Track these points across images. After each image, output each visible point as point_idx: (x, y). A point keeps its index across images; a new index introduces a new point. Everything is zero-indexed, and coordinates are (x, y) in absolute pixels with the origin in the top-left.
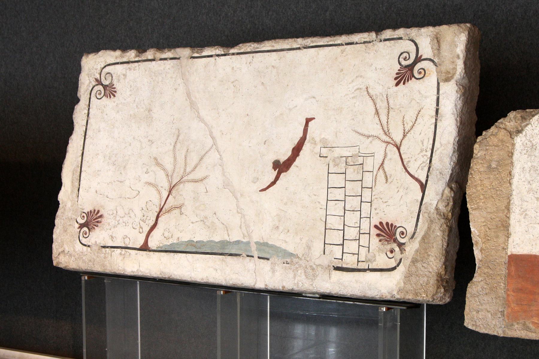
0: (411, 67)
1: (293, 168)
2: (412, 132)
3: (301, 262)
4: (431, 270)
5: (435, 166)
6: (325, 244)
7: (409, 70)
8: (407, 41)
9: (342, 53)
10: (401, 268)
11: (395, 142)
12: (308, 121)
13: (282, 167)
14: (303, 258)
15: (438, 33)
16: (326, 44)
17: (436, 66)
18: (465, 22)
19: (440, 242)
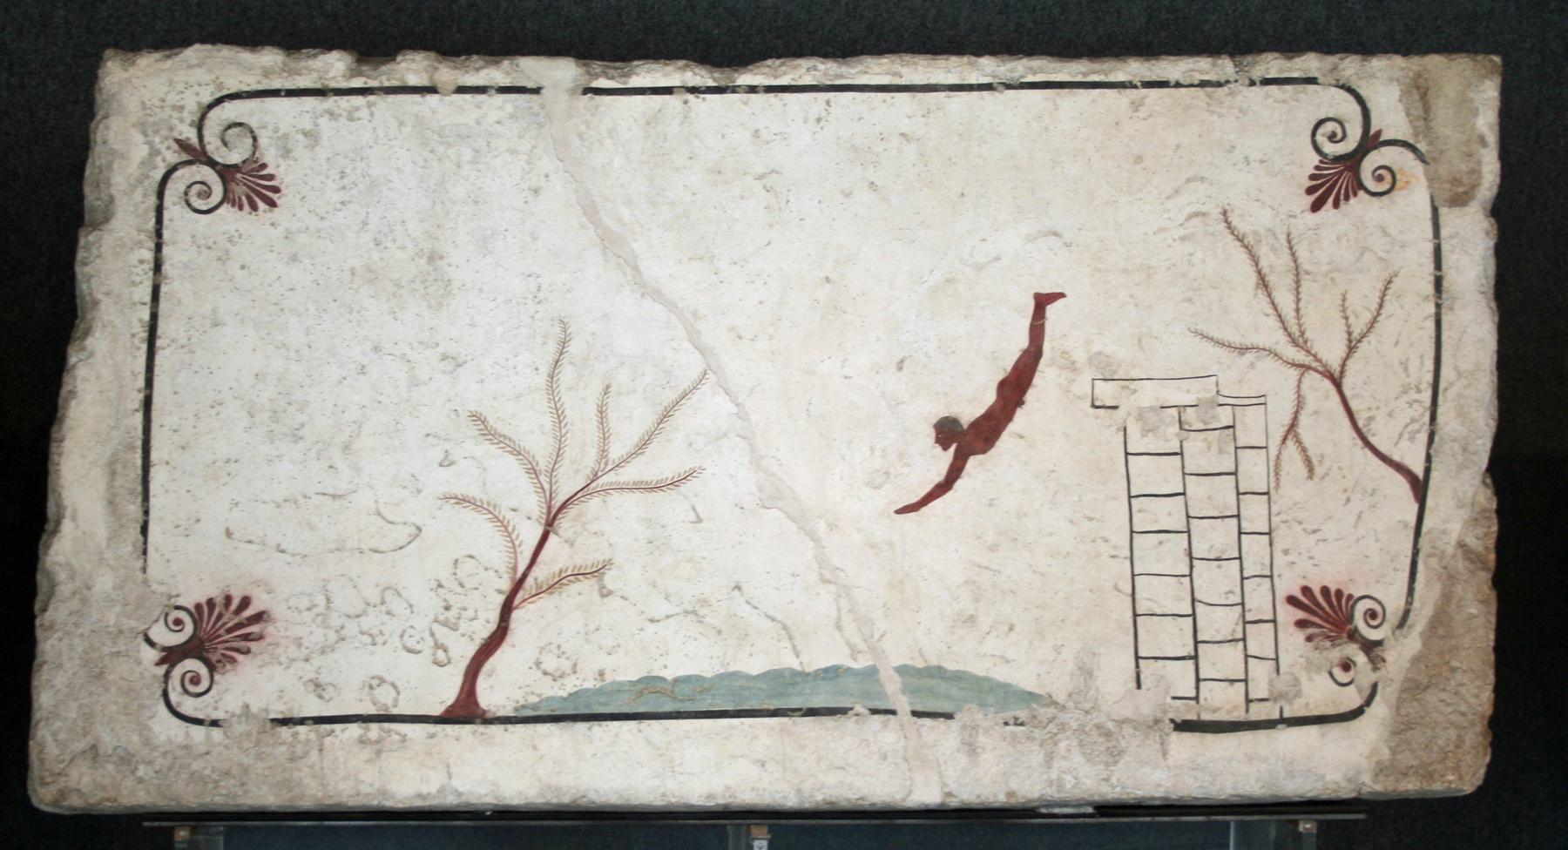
0: (1352, 161)
1: (1006, 441)
2: (1372, 337)
3: (1064, 717)
4: (1463, 708)
5: (1447, 429)
6: (1137, 658)
7: (1348, 168)
8: (1334, 90)
9: (1136, 110)
10: (1379, 710)
11: (1324, 366)
12: (1043, 302)
13: (966, 439)
14: (1071, 705)
15: (1418, 75)
16: (1079, 79)
17: (1423, 161)
18: (1489, 51)
19: (1481, 632)
